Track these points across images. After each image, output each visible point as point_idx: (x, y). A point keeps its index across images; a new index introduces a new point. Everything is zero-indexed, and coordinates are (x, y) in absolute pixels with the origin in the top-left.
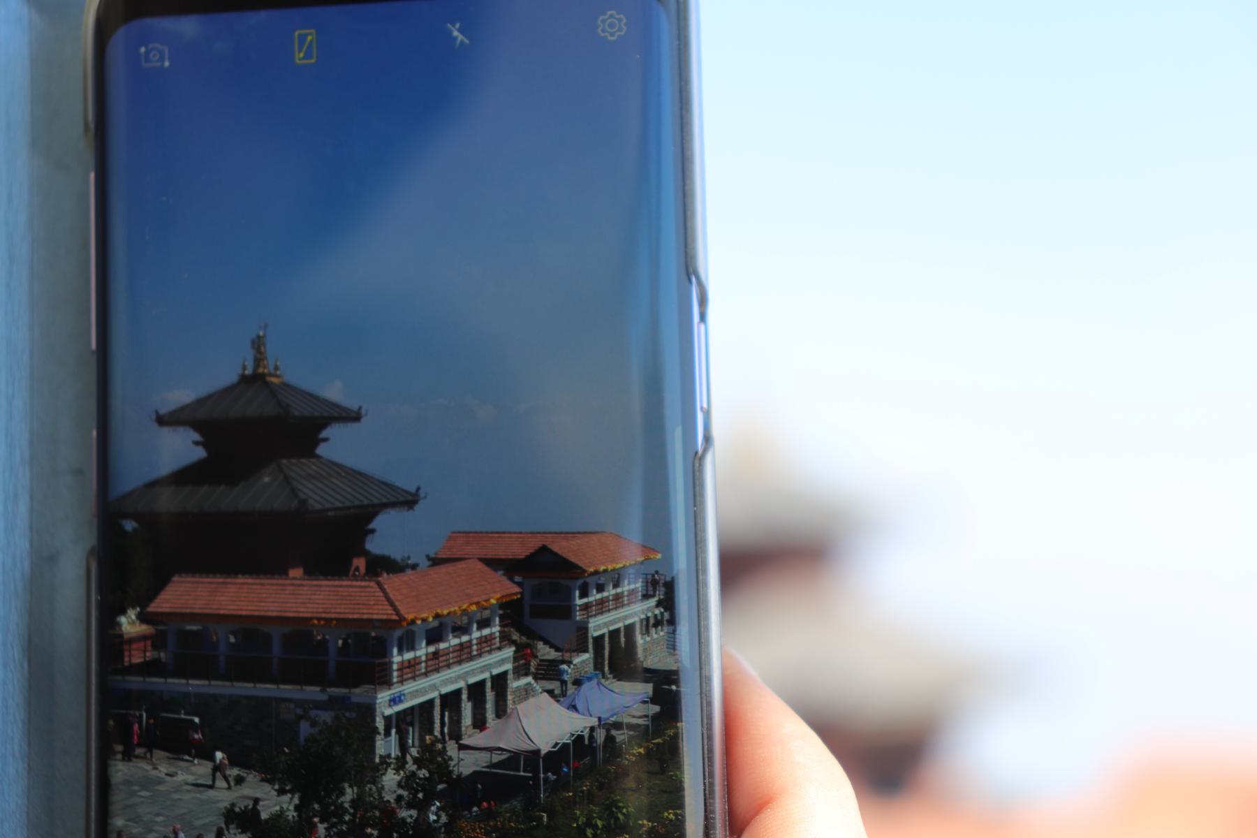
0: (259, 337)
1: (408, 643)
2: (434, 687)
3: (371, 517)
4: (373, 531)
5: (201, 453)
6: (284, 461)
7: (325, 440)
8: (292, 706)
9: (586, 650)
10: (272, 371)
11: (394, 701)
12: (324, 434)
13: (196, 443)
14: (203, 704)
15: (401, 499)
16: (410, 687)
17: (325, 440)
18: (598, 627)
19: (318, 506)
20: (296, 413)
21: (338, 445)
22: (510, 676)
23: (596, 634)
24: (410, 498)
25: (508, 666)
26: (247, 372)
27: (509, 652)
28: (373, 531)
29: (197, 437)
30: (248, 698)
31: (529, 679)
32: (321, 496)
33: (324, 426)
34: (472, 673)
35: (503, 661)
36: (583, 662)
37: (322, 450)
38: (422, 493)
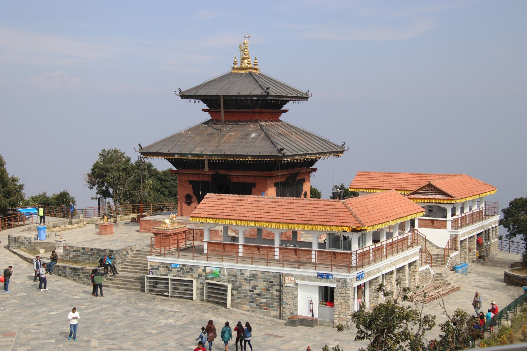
0: (244, 43)
1: (362, 241)
2: (379, 270)
3: (313, 162)
4: (315, 170)
5: (207, 117)
6: (263, 124)
7: (285, 111)
8: (293, 278)
9: (456, 249)
10: (253, 66)
11: (359, 278)
12: (285, 108)
13: (204, 110)
14: (233, 277)
15: (335, 150)
16: (367, 269)
17: (285, 111)
18: (463, 235)
19: (289, 154)
20: (273, 94)
21: (293, 114)
22: (418, 264)
23: (462, 239)
24: (339, 150)
25: (417, 258)
26: (236, 66)
27: (417, 249)
28: (315, 170)
29: (207, 108)
30: (263, 272)
31: (428, 266)
32: (293, 149)
33: (287, 101)
34: (398, 261)
35: (415, 254)
36: (456, 256)
37: (283, 117)
38: (346, 147)
